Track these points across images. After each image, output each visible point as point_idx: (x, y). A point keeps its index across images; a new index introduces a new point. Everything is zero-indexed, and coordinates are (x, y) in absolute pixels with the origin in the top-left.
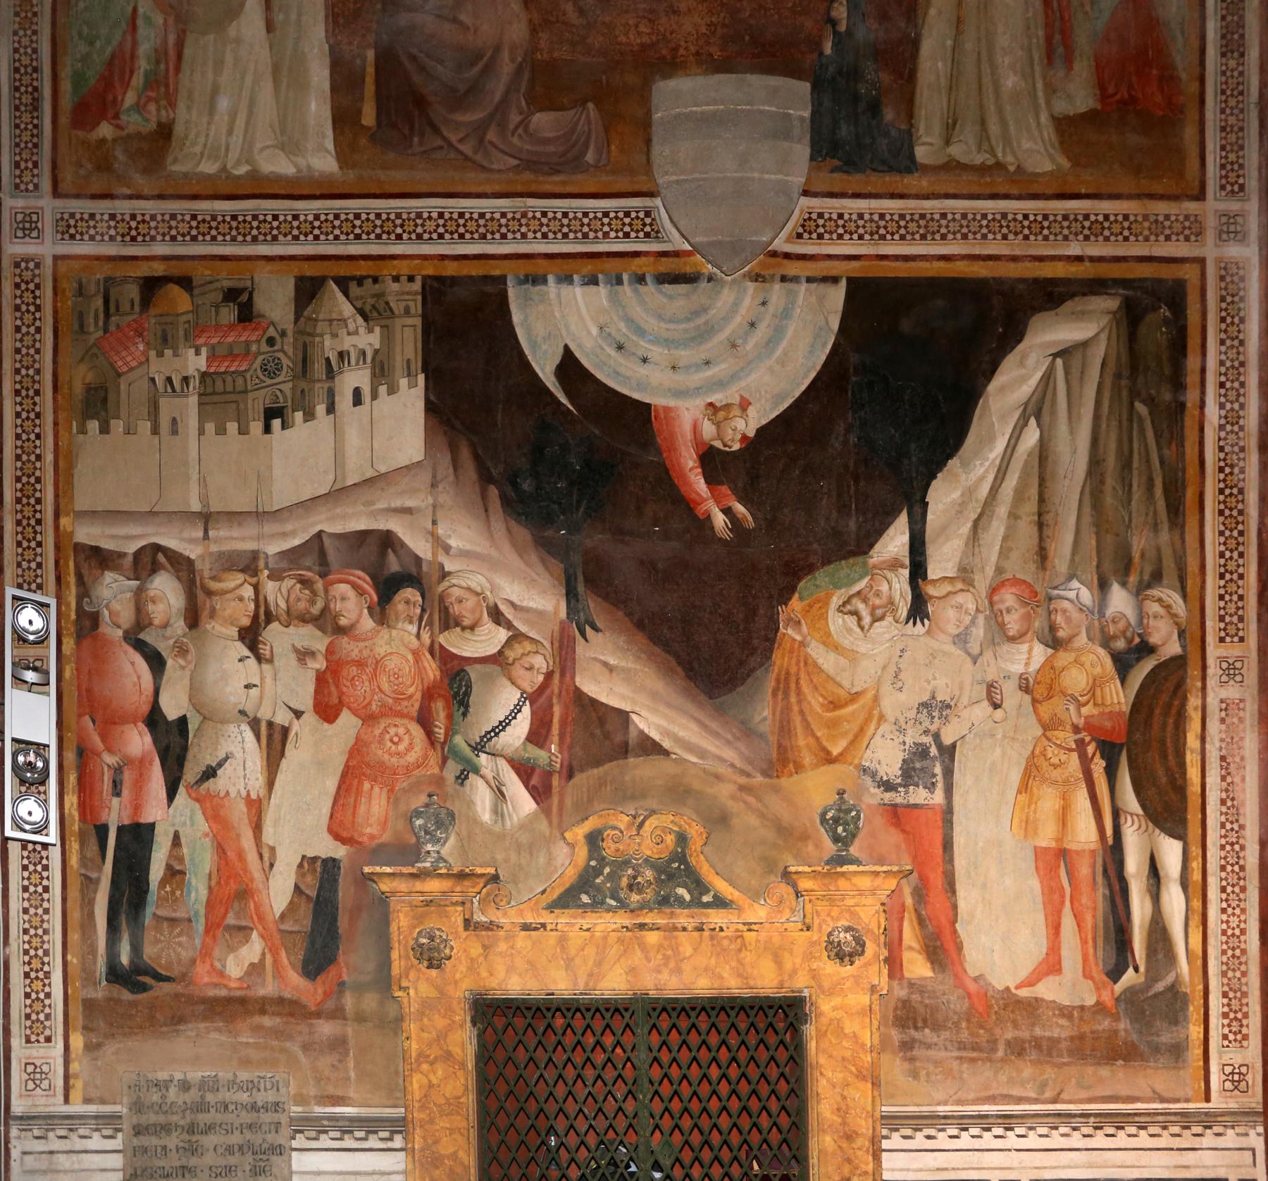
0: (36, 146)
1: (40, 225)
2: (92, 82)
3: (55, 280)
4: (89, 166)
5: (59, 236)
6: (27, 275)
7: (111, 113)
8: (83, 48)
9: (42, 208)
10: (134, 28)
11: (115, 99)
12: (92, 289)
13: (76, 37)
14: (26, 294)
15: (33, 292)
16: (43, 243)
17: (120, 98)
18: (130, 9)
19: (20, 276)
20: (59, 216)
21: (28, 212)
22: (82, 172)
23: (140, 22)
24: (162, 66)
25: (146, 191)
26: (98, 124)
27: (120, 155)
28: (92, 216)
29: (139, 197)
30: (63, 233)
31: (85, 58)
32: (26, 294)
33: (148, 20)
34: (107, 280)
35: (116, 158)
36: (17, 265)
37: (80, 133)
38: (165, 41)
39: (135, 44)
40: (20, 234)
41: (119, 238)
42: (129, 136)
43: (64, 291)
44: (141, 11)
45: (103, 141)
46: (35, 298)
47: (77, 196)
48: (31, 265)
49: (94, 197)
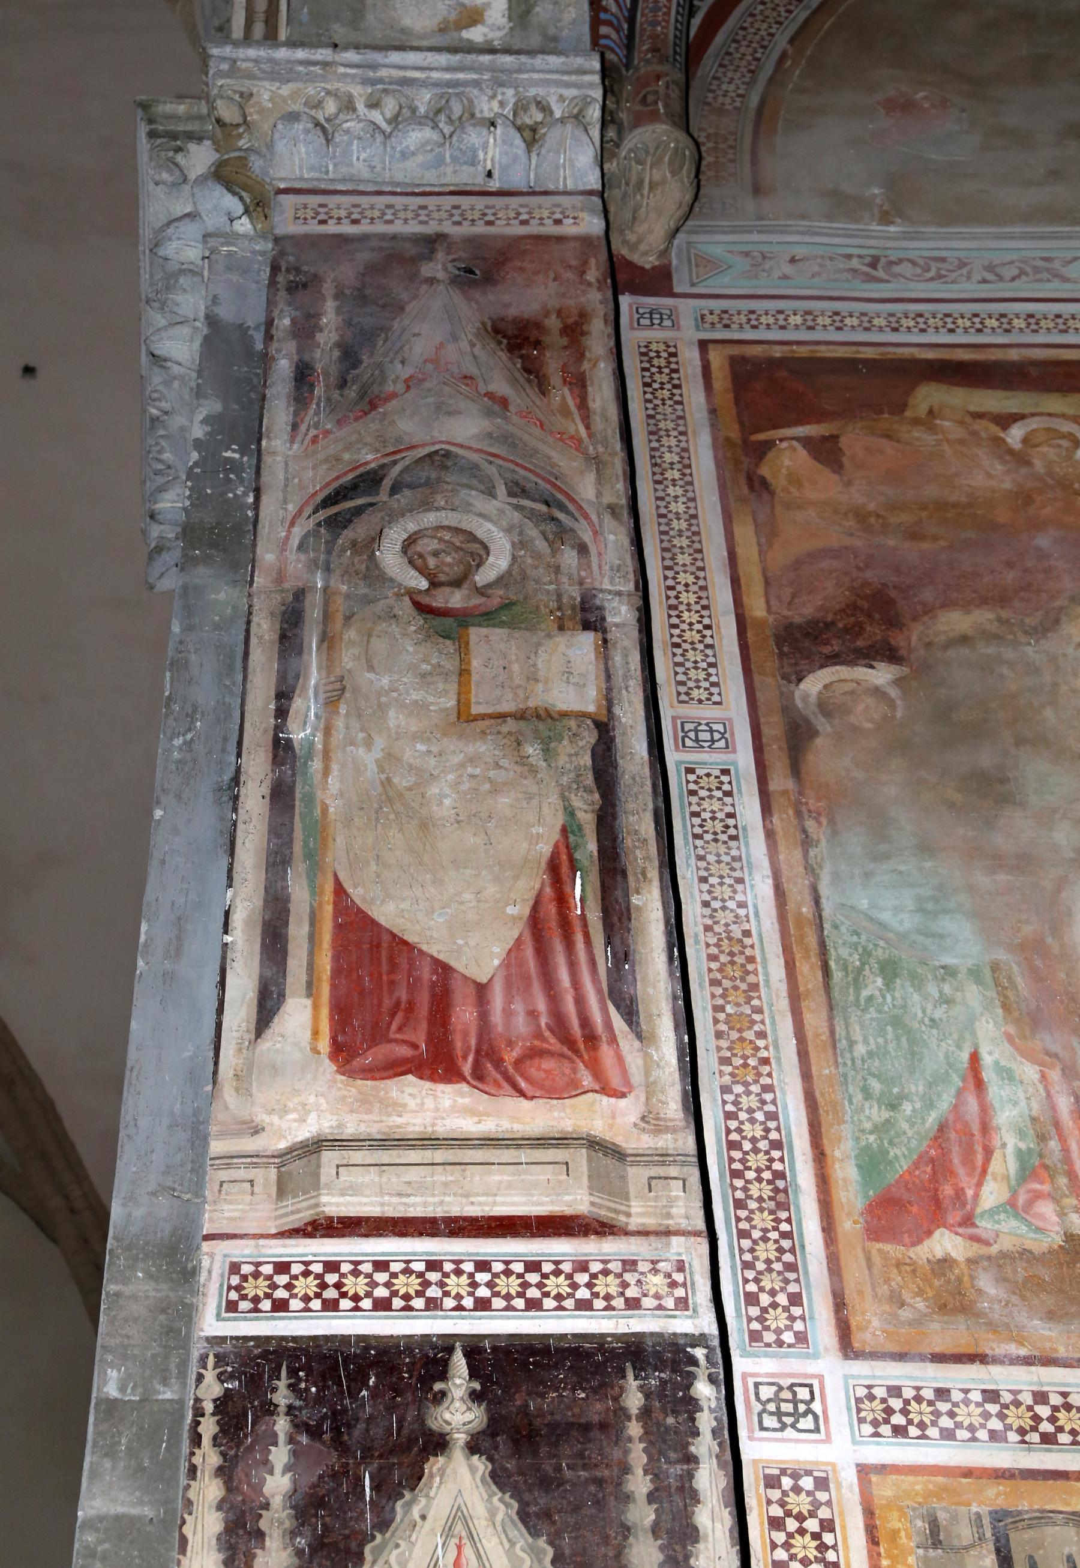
0: (791, 1267)
1: (816, 1406)
2: (904, 1165)
3: (869, 1513)
4: (920, 1304)
5: (868, 1429)
6: (800, 1503)
7: (954, 1217)
8: (876, 1114)
9: (821, 1378)
10: (979, 1085)
11: (959, 1193)
12: (965, 1533)
13: (858, 1097)
14: (798, 1541)
15: (816, 1536)
16: (828, 1439)
17: (970, 1193)
18: (965, 1056)
19: (782, 1504)
20: (862, 1392)
21: (786, 1382)
22: (905, 1314)
23: (988, 1075)
24: (1054, 1144)
25: (1062, 1352)
26: (929, 1233)
27: (987, 1283)
28: (942, 1393)
29: (1048, 1361)
30: (875, 1423)
31: (882, 1129)
32: (798, 1541)
33: (1008, 1075)
34: (999, 1516)
35: (980, 1291)
36: (772, 1482)
37: (893, 1249)
38: (1053, 1108)
39: (985, 1110)
40: (770, 1422)
41: (1013, 1437)
42: (1003, 1255)
43: (894, 1534)
44: (987, 1060)
45: (946, 1263)
46: (823, 1548)
47: (901, 1357)
48: (807, 1483)
49: (939, 1358)
